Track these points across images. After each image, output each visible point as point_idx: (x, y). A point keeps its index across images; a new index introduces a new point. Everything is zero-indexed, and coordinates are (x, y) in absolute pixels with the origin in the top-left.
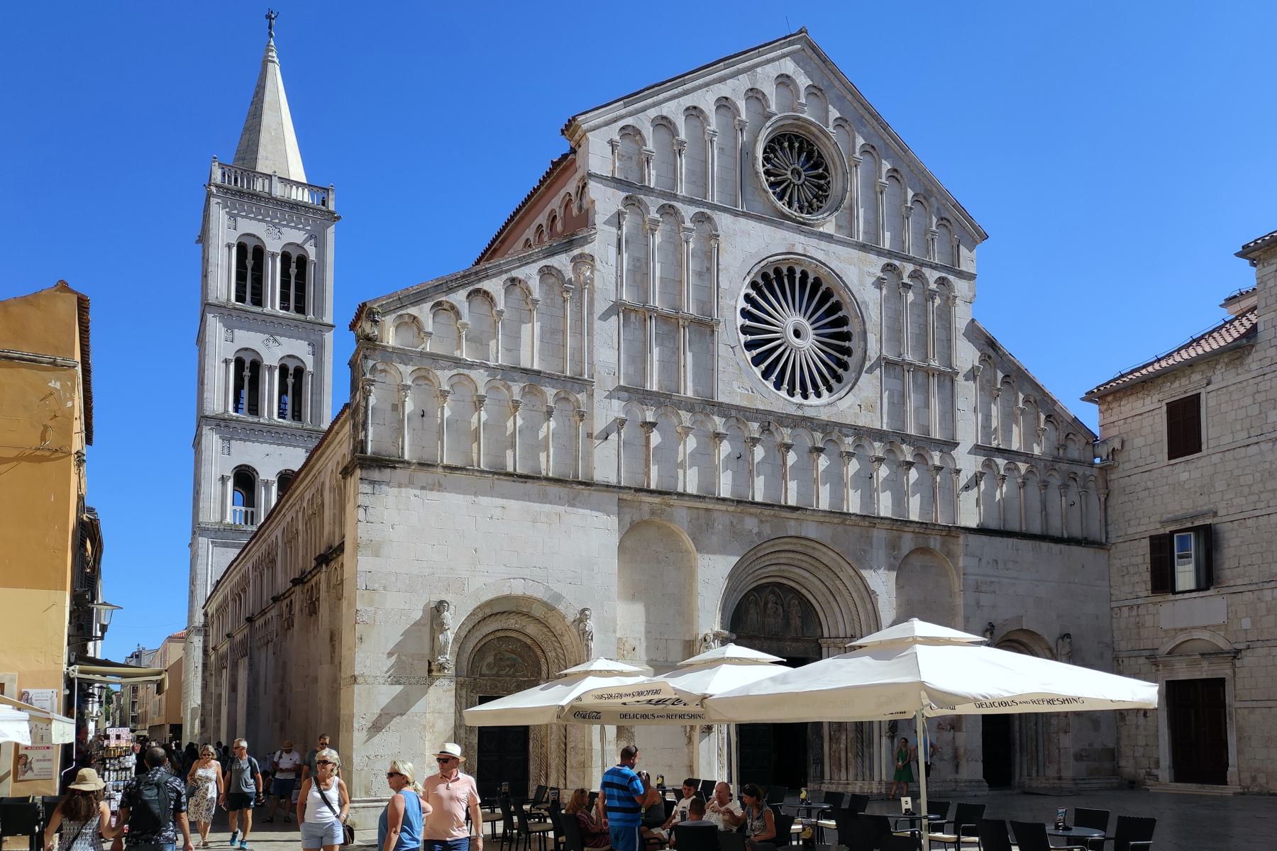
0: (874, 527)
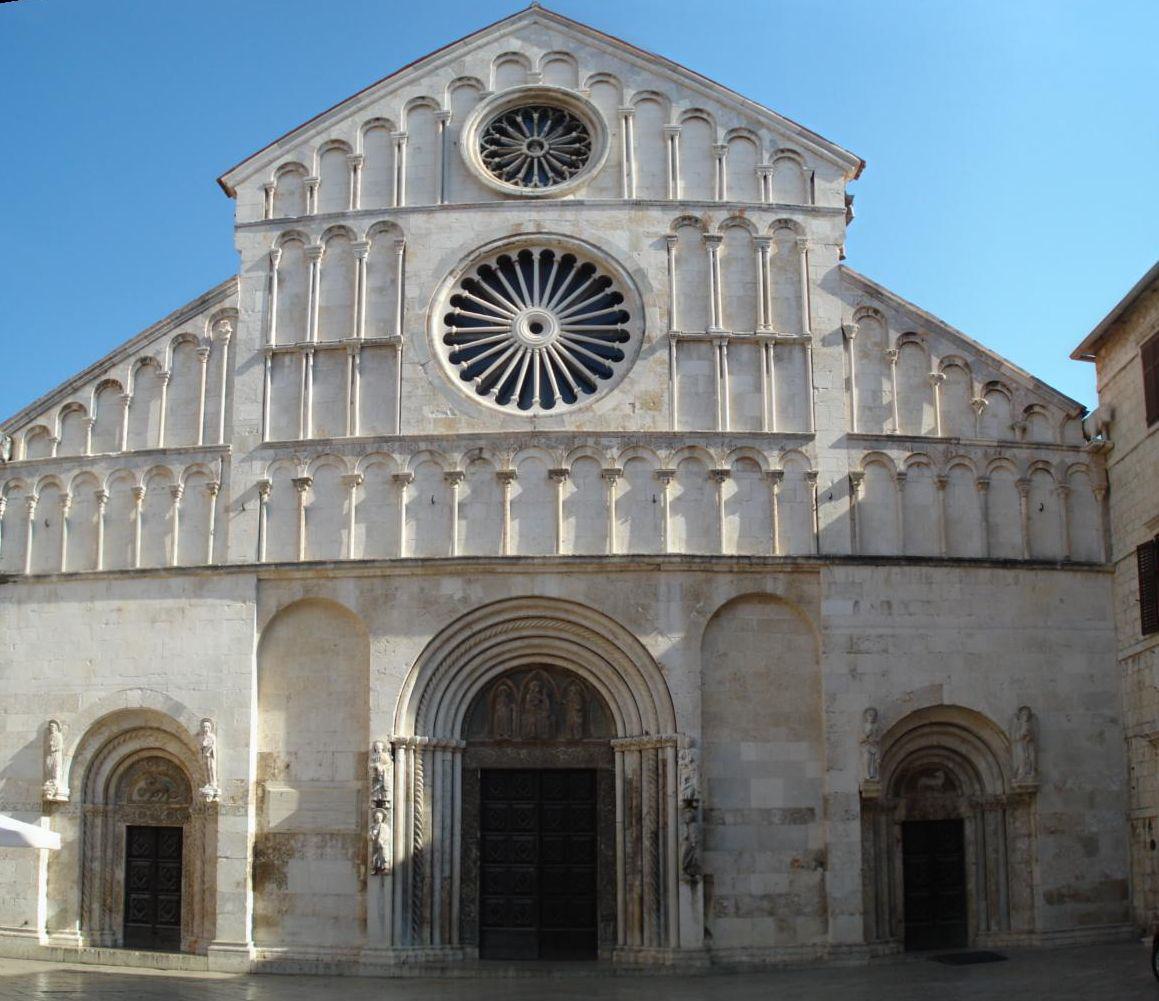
0: (659, 570)
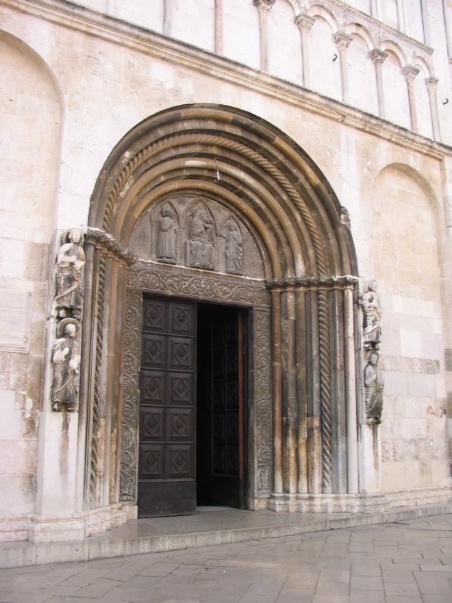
0: (342, 122)
